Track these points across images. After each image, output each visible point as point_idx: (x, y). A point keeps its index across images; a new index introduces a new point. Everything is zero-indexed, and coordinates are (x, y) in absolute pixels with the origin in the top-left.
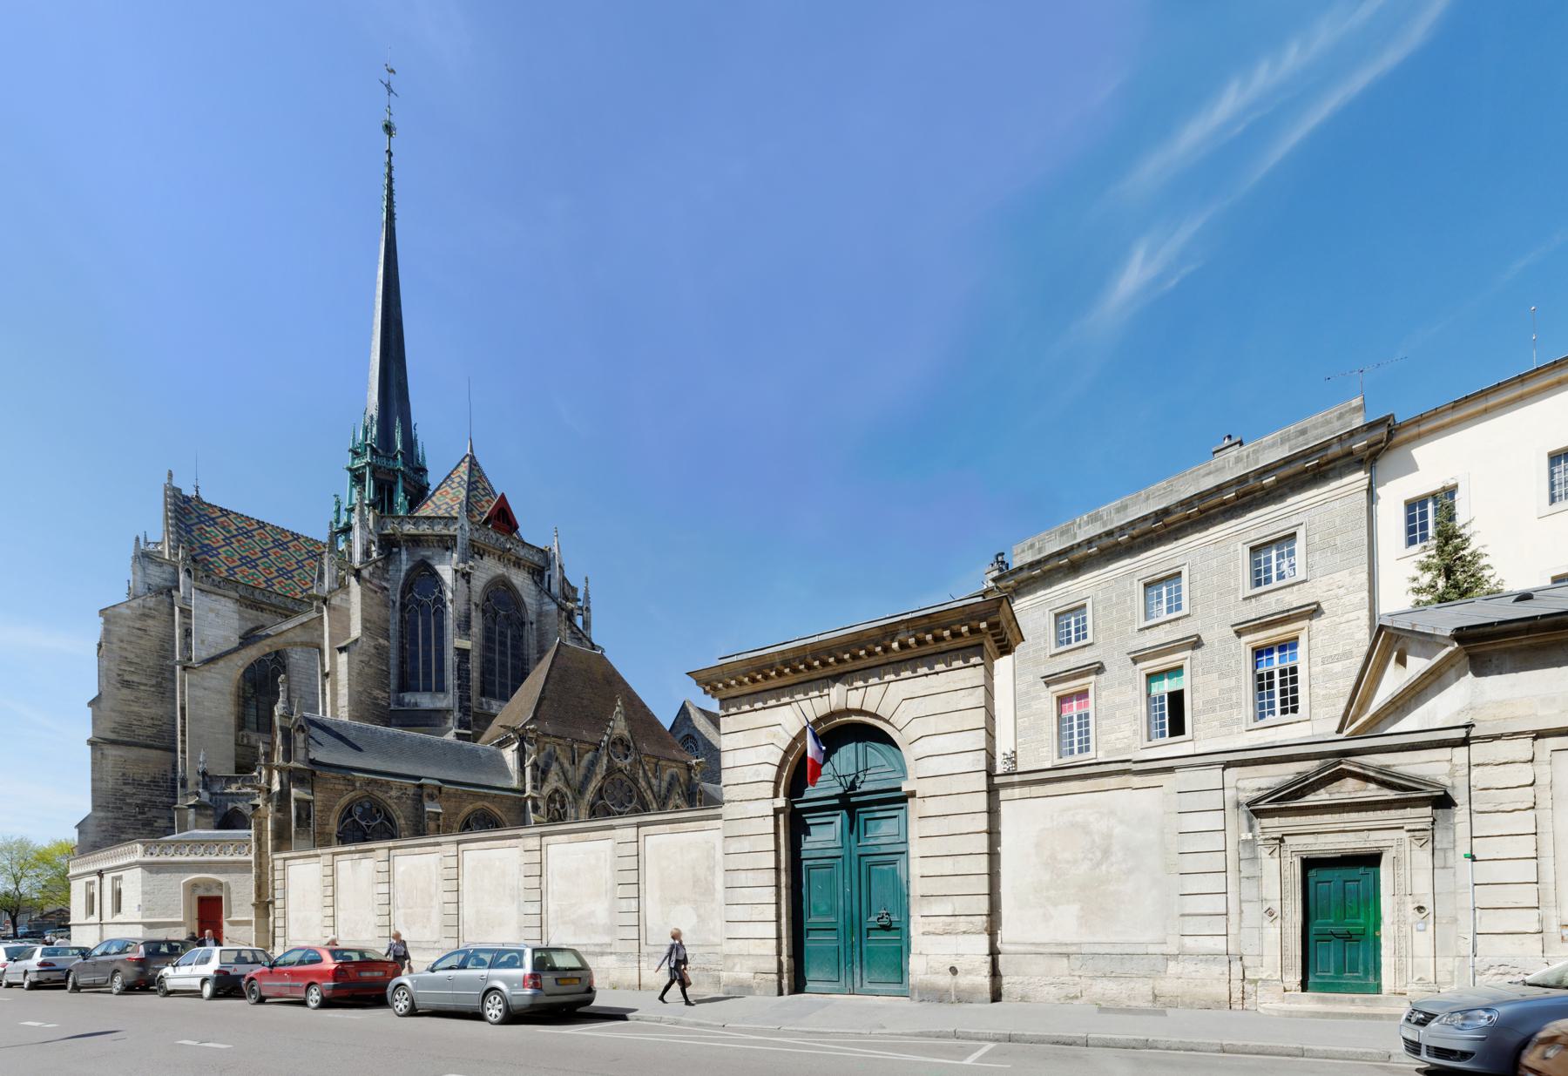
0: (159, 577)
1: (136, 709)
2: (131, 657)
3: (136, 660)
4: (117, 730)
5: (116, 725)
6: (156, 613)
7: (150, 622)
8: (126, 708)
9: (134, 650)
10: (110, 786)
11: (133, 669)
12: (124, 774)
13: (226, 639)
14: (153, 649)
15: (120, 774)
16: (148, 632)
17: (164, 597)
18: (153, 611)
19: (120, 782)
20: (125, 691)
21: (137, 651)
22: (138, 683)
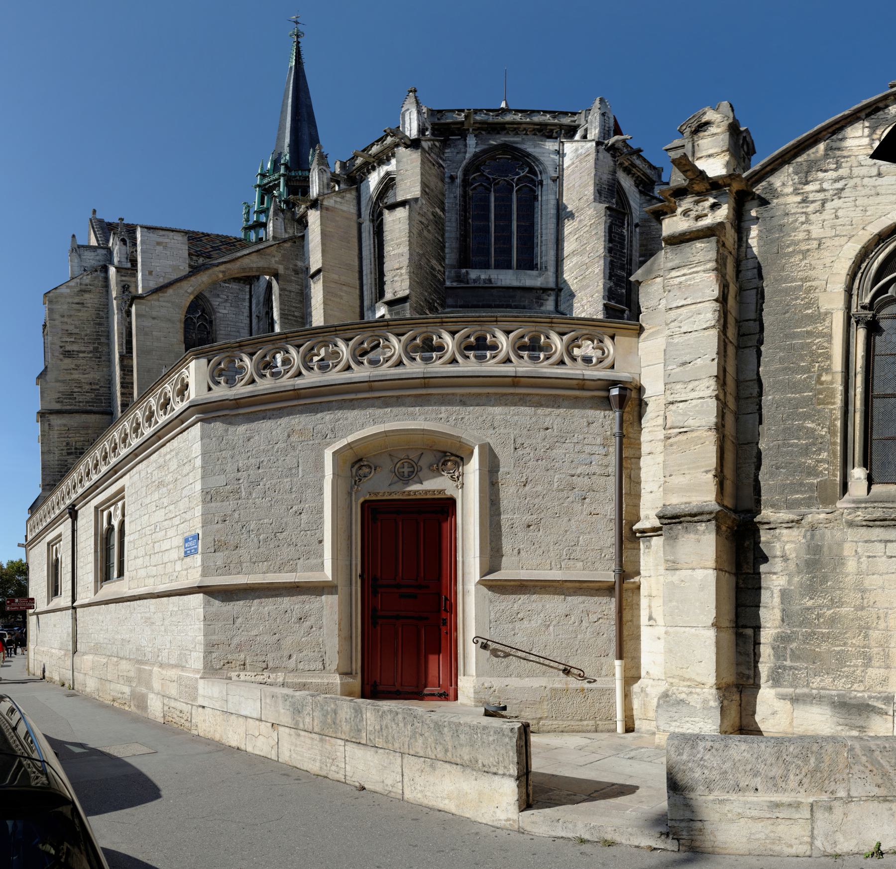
0: (93, 259)
1: (76, 376)
2: (71, 328)
3: (77, 331)
4: (61, 400)
5: (60, 395)
6: (91, 287)
7: (87, 296)
8: (68, 377)
9: (73, 322)
10: (57, 458)
11: (73, 340)
12: (68, 444)
13: (175, 268)
14: (90, 319)
15: (64, 444)
16: (85, 305)
17: (99, 273)
18: (89, 287)
19: (64, 452)
20: (67, 361)
21: (77, 323)
22: (78, 352)
